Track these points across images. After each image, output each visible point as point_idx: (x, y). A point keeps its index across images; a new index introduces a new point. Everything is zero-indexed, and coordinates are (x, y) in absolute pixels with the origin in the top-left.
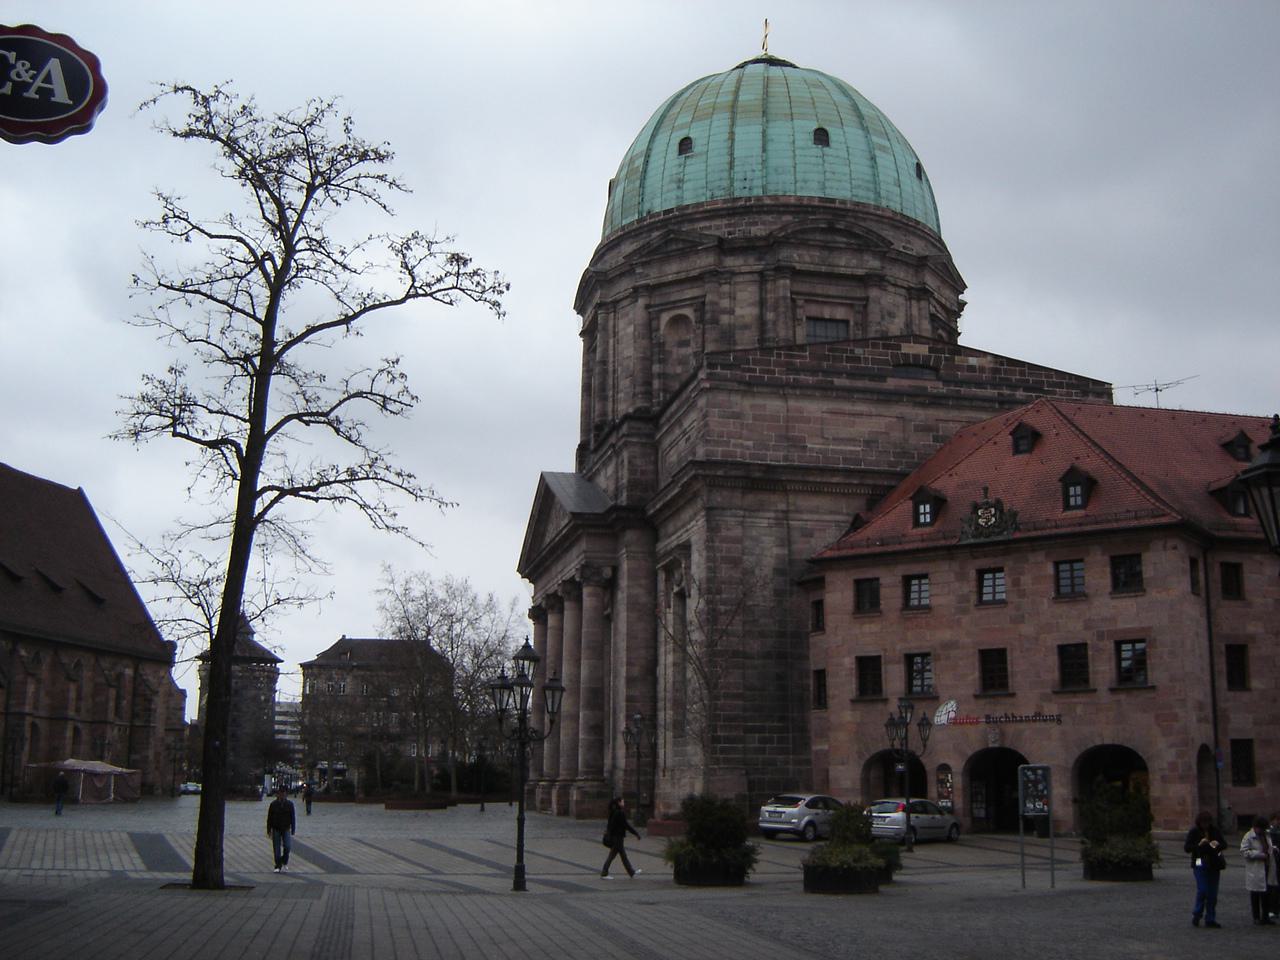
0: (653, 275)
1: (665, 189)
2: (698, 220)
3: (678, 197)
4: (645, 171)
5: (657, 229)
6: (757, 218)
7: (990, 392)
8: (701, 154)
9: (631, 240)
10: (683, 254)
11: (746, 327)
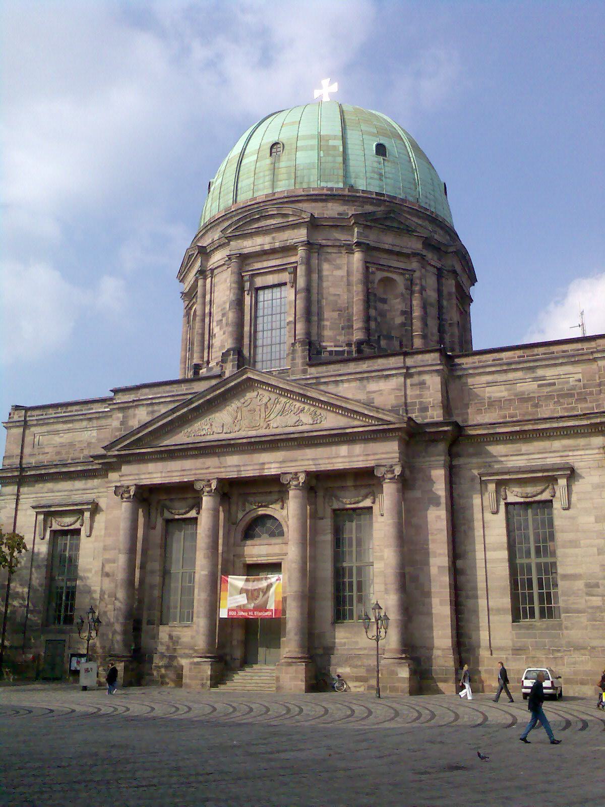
0: (372, 238)
1: (368, 175)
5: (372, 204)
11: (431, 305)
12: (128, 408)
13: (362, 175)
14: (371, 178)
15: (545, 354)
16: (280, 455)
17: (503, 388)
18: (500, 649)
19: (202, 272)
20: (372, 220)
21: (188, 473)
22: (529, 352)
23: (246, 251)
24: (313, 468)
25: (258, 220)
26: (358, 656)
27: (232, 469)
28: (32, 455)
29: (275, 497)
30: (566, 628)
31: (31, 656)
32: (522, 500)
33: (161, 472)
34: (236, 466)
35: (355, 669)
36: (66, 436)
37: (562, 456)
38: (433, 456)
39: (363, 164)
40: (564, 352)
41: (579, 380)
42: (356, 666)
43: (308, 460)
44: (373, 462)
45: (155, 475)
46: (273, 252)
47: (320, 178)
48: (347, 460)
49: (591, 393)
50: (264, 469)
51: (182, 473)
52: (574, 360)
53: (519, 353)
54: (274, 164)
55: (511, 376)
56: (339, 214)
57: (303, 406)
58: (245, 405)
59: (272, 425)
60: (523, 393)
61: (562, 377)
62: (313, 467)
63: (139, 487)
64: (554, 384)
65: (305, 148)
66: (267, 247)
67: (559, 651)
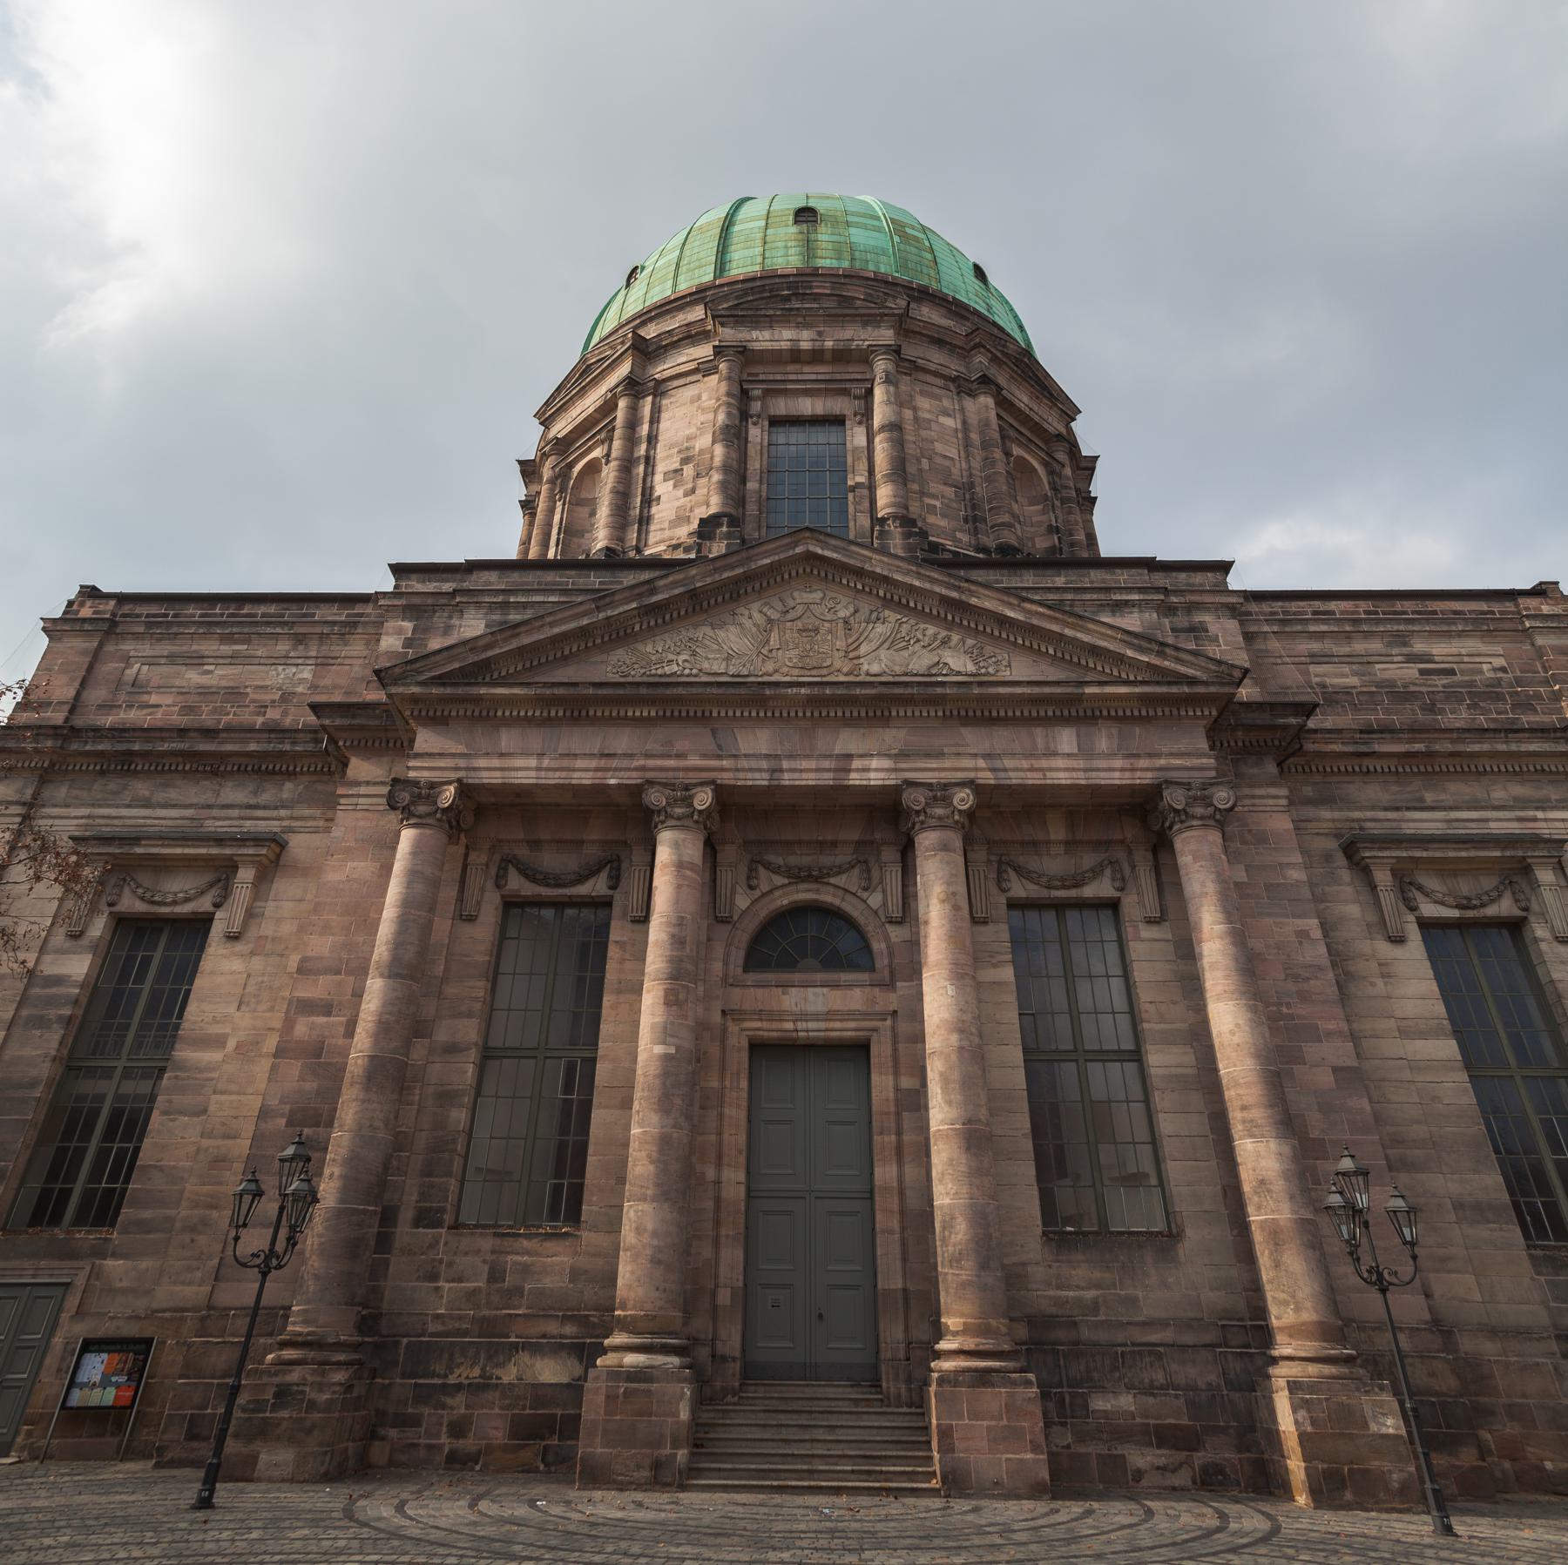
12: (434, 609)
15: (1418, 613)
16: (894, 737)
17: (1346, 669)
19: (634, 387)
21: (625, 763)
22: (1383, 606)
23: (757, 346)
24: (987, 778)
26: (1154, 1352)
27: (753, 764)
29: (843, 857)
32: (1456, 913)
33: (541, 755)
34: (757, 756)
35: (1151, 1400)
37: (1520, 820)
38: (1261, 786)
40: (1455, 612)
41: (1503, 670)
42: (1150, 1390)
43: (975, 755)
44: (1149, 775)
45: (519, 762)
46: (816, 356)
48: (1081, 764)
50: (850, 770)
51: (603, 763)
52: (1484, 627)
53: (1364, 605)
55: (1359, 647)
57: (944, 633)
58: (790, 616)
59: (865, 667)
60: (1391, 683)
61: (1466, 659)
62: (989, 774)
64: (1452, 672)
66: (805, 345)
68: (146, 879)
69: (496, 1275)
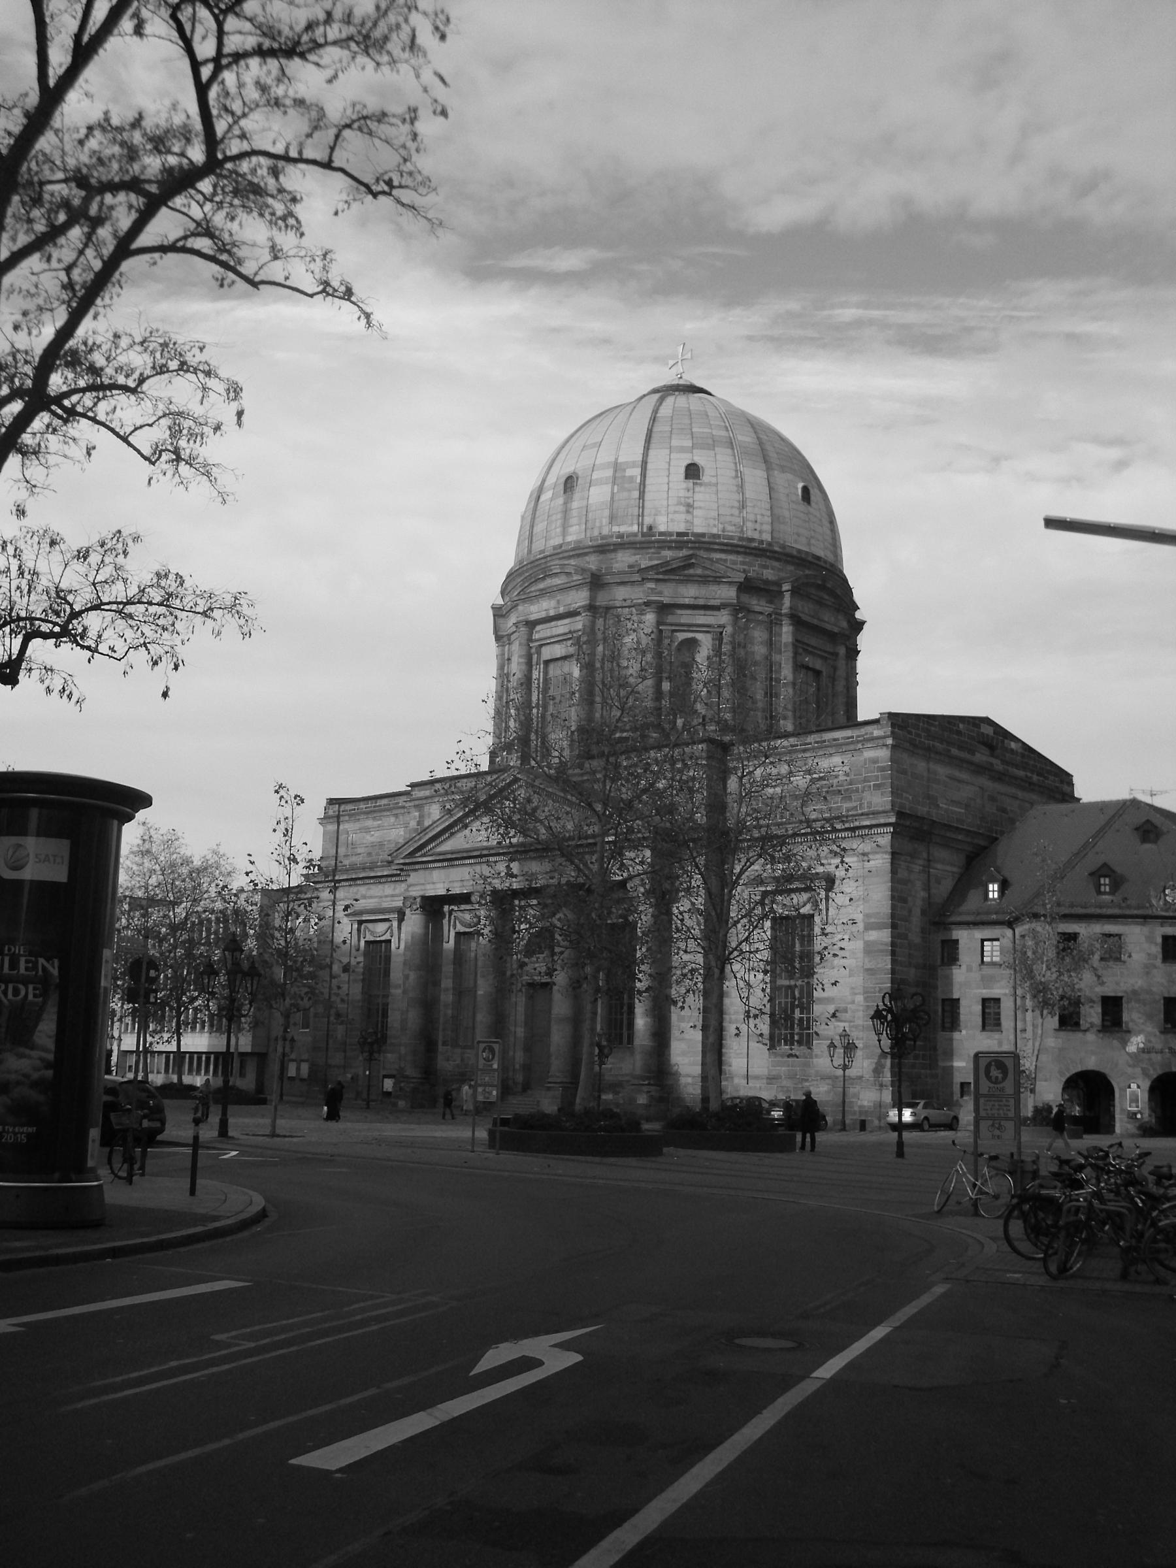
0: (667, 593)
1: (671, 509)
2: (716, 551)
3: (687, 522)
4: (643, 483)
5: (670, 548)
6: (769, 562)
7: (1021, 773)
8: (710, 484)
9: (633, 551)
10: (704, 580)
13: (663, 511)
14: (675, 512)
18: (757, 1078)
20: (665, 573)
23: (533, 617)
25: (543, 579)
28: (346, 856)
30: (816, 1056)
31: (349, 1076)
36: (377, 834)
39: (665, 496)
40: (835, 740)
47: (612, 519)
49: (857, 790)
54: (565, 503)
56: (630, 566)
63: (424, 898)
65: (600, 482)
66: (552, 613)
67: (807, 1080)
68: (370, 925)
69: (462, 1060)
